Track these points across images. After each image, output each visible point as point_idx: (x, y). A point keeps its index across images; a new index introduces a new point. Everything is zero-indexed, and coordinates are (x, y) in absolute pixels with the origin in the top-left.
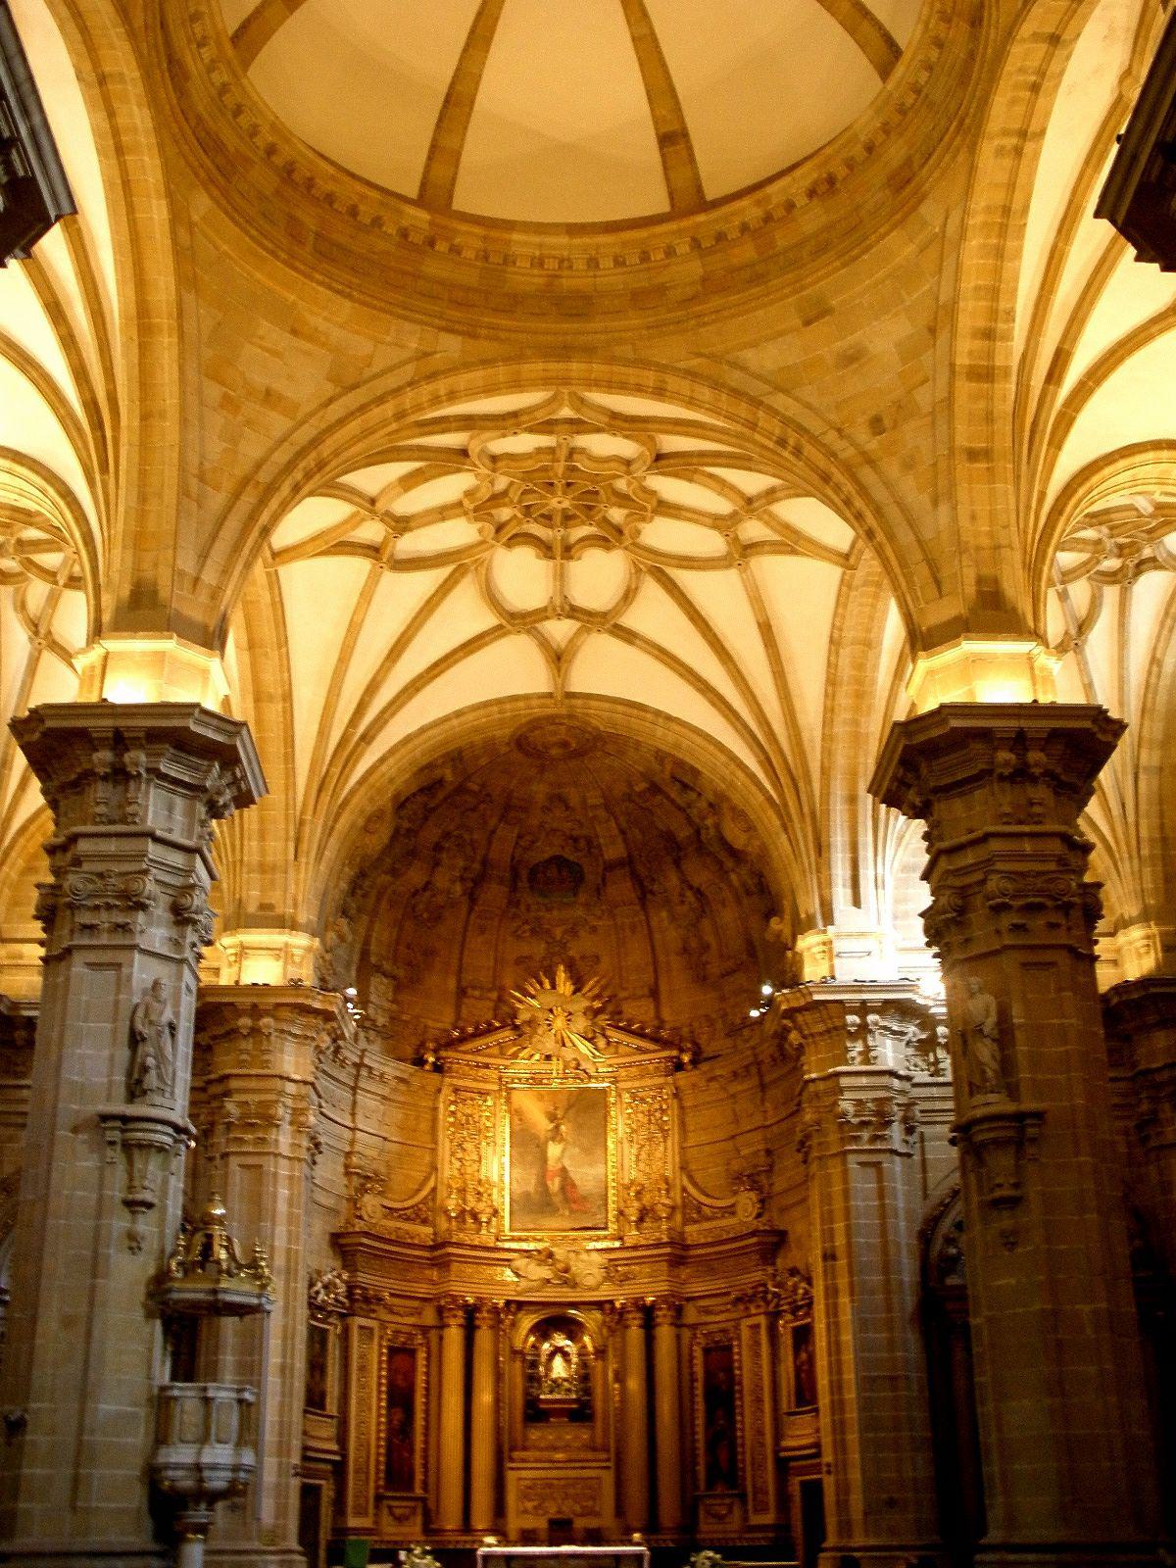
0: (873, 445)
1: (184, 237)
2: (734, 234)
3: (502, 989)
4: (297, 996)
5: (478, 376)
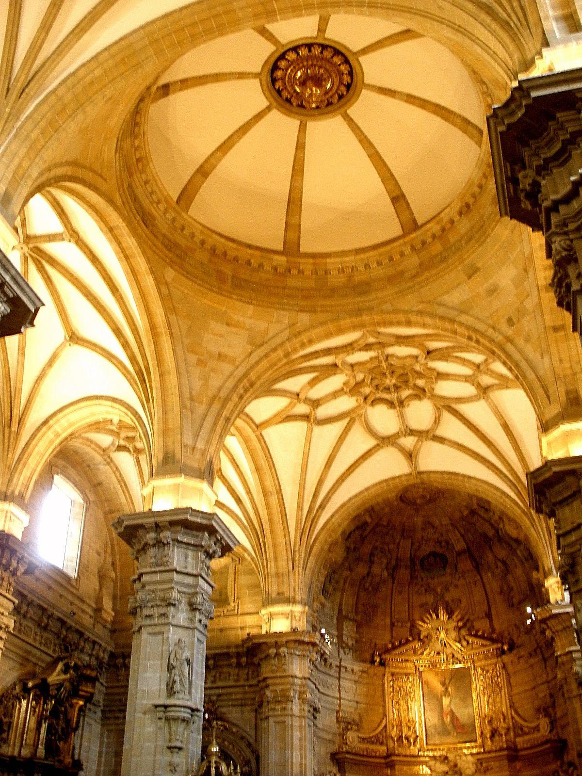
0: (510, 332)
1: (164, 290)
2: (429, 240)
3: (414, 621)
5: (320, 330)
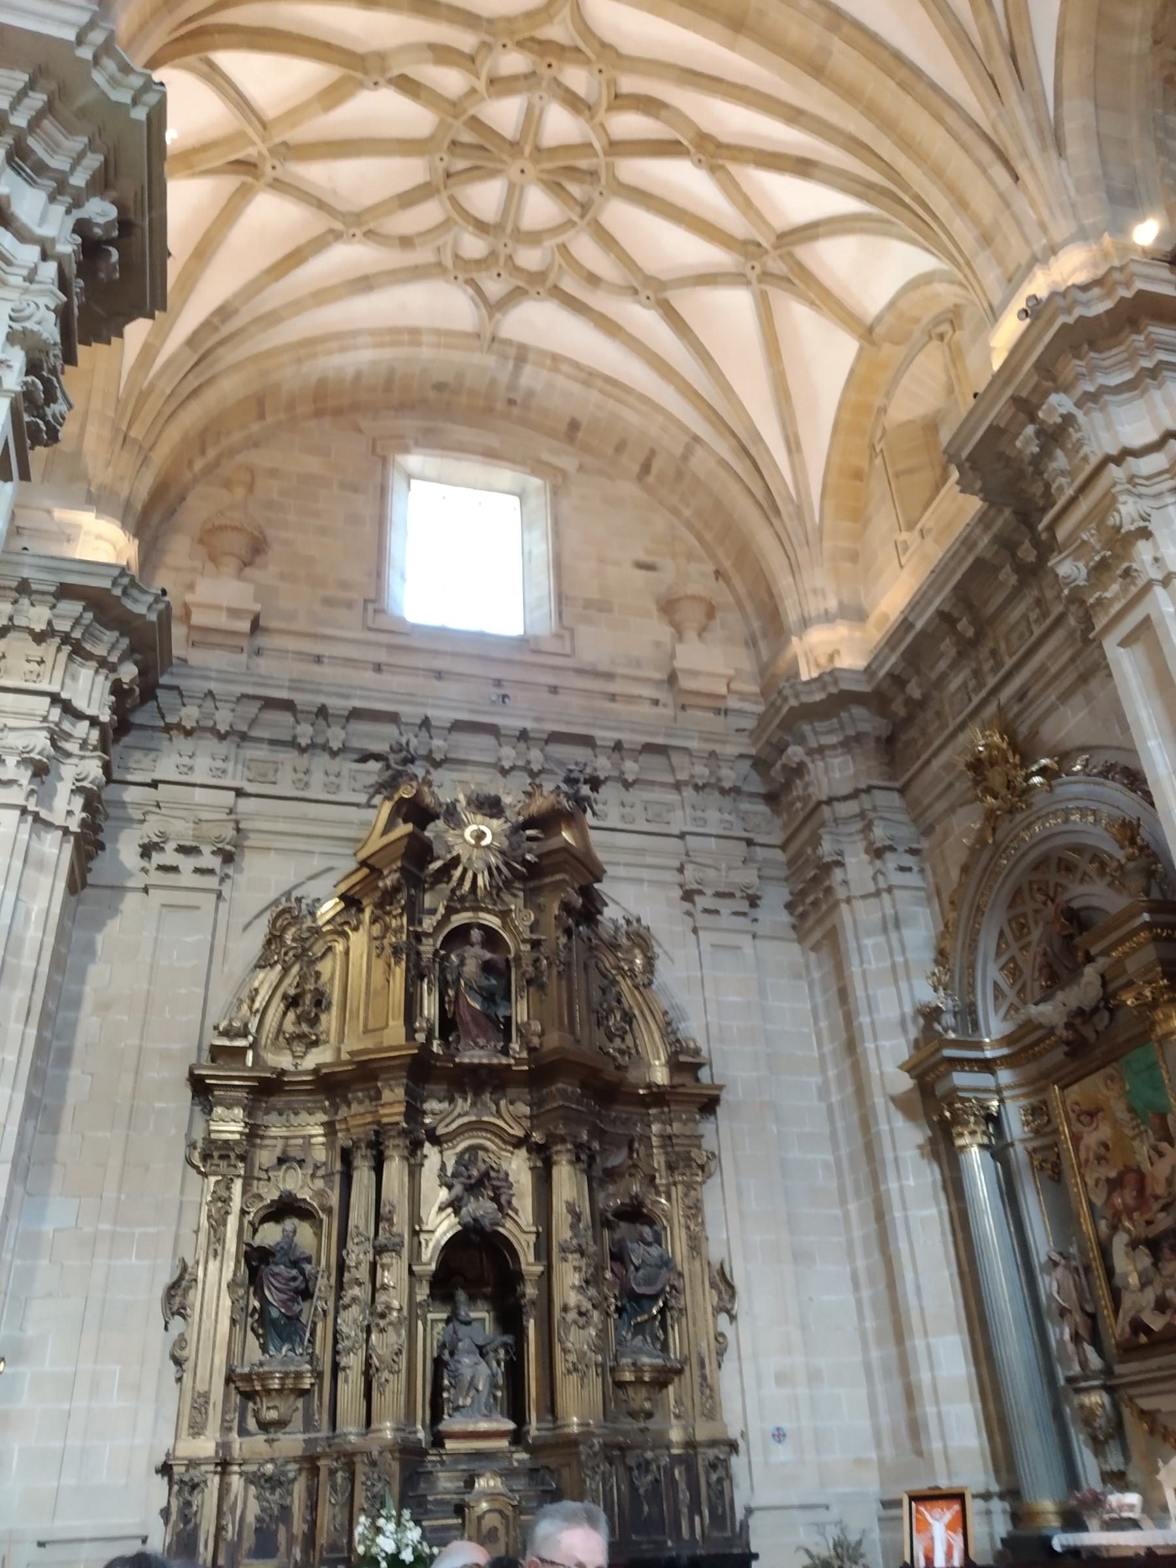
4: (1051, 321)
